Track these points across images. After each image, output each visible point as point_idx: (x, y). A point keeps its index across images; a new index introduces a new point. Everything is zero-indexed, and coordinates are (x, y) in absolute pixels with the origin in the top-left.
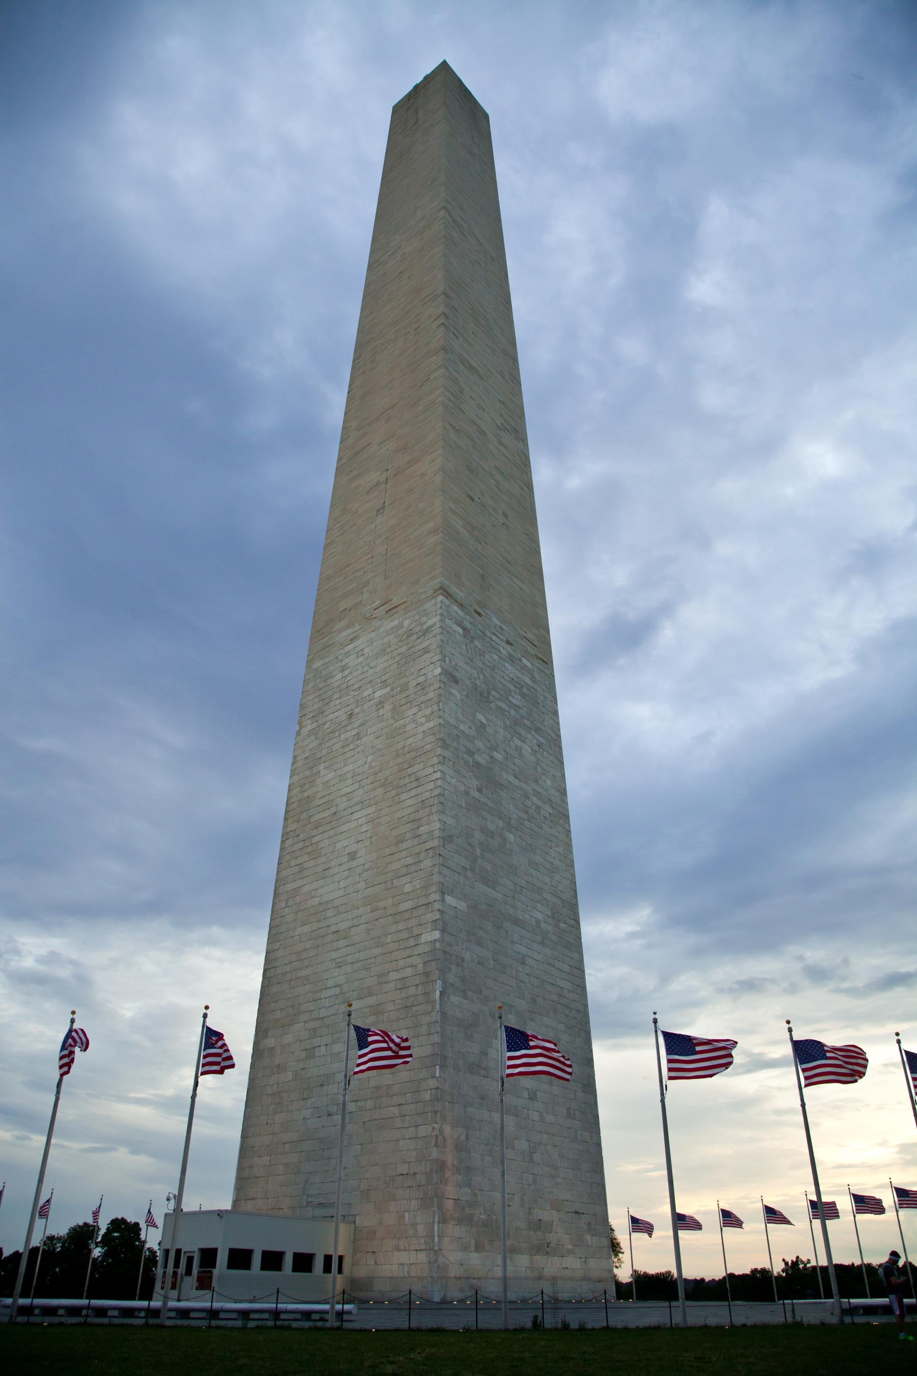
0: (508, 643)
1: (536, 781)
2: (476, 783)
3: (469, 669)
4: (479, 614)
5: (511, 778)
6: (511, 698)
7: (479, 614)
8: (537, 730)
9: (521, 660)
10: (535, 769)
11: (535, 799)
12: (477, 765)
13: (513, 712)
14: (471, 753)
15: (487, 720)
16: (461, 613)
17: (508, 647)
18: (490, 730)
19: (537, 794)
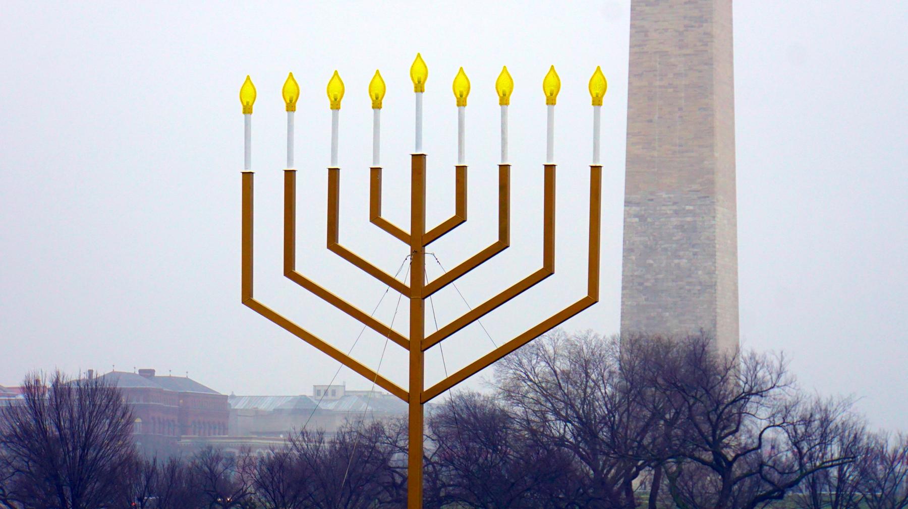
0: (675, 203)
1: (689, 276)
2: (644, 297)
3: (642, 239)
4: (652, 200)
5: (670, 284)
6: (674, 238)
7: (652, 200)
8: (693, 246)
9: (684, 209)
10: (690, 270)
11: (687, 287)
12: (647, 287)
13: (674, 246)
14: (641, 284)
15: (654, 260)
16: (637, 209)
17: (675, 207)
18: (655, 265)
19: (689, 283)
